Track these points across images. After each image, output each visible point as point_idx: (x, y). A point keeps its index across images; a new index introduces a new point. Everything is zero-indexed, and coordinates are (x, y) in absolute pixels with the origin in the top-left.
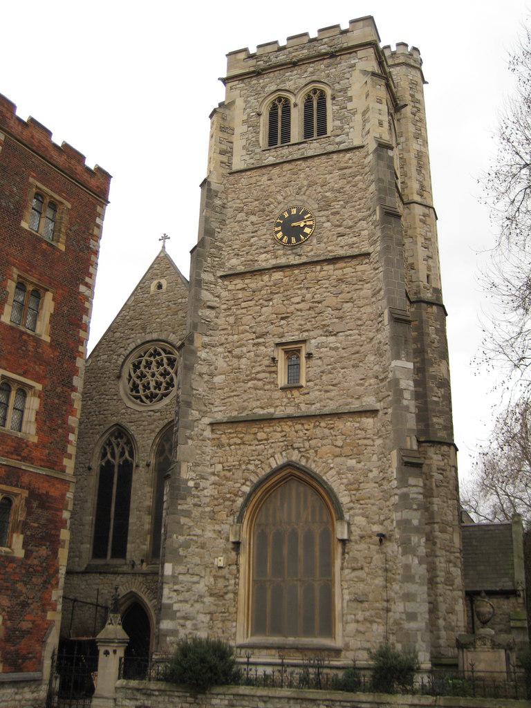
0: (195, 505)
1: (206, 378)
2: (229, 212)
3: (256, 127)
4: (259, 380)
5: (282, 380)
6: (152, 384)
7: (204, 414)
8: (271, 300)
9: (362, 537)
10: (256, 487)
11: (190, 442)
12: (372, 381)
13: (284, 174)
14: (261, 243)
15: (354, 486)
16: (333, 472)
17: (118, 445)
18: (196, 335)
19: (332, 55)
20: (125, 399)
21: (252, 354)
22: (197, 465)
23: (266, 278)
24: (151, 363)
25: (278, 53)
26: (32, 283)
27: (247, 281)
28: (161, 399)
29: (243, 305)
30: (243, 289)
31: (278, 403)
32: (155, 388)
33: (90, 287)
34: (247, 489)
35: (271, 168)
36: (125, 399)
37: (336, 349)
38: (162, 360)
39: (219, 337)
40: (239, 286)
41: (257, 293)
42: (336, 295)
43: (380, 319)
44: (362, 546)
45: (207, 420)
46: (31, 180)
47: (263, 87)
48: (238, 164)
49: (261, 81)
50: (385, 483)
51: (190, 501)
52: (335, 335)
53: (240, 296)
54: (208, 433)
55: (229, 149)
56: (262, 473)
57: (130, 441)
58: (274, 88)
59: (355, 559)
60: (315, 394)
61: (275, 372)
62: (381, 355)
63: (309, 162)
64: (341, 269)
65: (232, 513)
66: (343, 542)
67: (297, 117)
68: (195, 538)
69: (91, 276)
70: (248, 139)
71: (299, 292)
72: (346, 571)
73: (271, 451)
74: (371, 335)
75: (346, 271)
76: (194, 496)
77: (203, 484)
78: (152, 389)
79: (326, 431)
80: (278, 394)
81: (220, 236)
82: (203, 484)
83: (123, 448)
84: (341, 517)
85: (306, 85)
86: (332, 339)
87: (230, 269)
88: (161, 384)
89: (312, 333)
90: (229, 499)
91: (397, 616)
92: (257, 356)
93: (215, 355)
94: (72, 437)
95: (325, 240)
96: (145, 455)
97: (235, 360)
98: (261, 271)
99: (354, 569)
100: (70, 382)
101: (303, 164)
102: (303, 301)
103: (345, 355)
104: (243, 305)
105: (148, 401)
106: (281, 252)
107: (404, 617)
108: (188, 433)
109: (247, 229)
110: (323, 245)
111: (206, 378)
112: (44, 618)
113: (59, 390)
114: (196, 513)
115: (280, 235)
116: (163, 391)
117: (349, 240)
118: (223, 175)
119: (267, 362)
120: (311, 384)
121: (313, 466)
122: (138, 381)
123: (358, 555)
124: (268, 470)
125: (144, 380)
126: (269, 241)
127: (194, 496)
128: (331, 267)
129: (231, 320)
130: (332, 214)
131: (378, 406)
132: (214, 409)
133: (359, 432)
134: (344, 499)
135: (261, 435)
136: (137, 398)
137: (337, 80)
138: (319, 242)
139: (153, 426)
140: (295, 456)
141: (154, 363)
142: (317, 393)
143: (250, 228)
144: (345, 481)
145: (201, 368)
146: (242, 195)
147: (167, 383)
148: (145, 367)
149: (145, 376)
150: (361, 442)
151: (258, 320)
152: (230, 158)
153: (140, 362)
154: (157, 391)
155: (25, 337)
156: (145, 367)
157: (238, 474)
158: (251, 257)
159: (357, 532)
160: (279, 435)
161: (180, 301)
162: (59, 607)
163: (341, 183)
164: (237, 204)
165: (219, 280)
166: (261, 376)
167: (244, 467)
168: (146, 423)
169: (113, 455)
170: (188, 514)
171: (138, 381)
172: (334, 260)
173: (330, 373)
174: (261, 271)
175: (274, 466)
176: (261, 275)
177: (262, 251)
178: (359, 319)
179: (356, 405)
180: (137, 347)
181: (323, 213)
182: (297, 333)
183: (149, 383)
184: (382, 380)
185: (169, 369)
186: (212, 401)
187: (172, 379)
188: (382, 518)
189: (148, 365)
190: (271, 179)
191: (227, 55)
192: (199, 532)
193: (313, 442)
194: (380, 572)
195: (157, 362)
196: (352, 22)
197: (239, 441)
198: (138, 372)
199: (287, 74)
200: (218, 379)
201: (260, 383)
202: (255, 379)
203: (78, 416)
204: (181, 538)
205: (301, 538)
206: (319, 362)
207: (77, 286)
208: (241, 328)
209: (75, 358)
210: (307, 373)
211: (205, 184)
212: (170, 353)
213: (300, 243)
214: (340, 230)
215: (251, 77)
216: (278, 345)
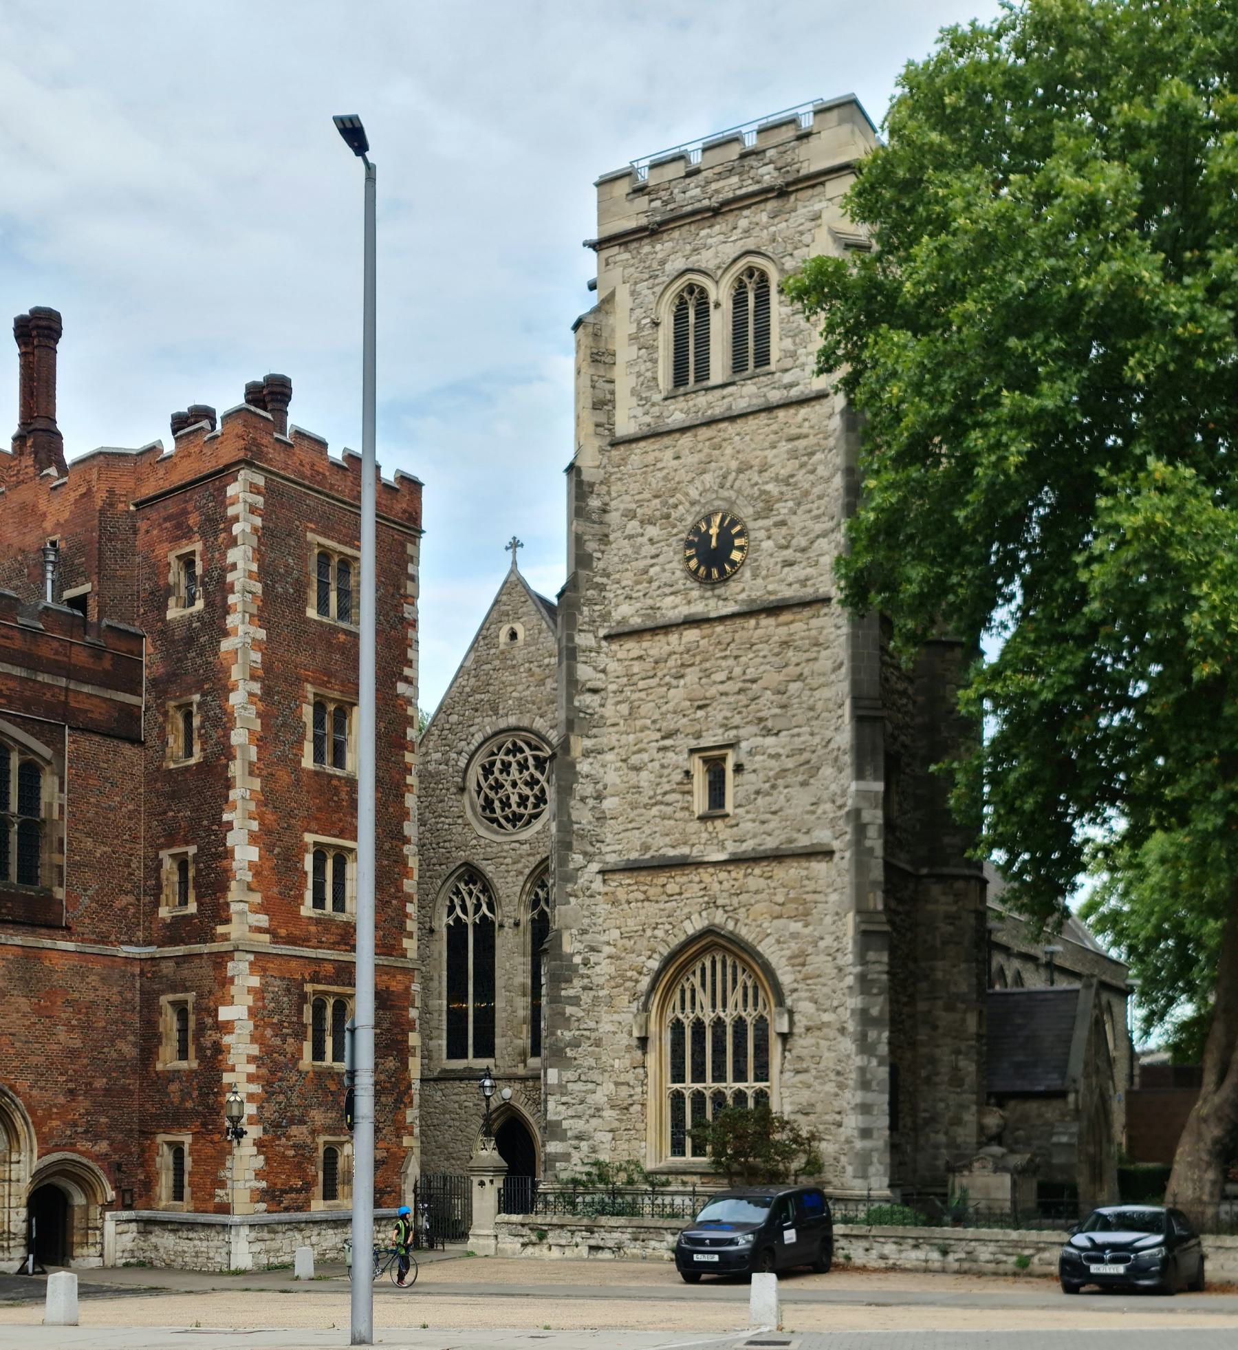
0: (584, 988)
1: (591, 802)
2: (614, 518)
3: (652, 348)
4: (668, 804)
5: (700, 801)
6: (514, 799)
7: (589, 857)
8: (682, 676)
9: (808, 1029)
10: (668, 961)
11: (572, 900)
12: (828, 806)
13: (700, 446)
14: (666, 577)
15: (800, 960)
16: (771, 940)
17: (470, 893)
18: (572, 739)
19: (782, 193)
20: (475, 823)
21: (656, 764)
22: (584, 932)
23: (673, 638)
24: (510, 764)
25: (688, 181)
26: (333, 700)
27: (645, 644)
28: (529, 822)
29: (641, 685)
30: (640, 658)
31: (694, 839)
32: (519, 805)
33: (410, 681)
34: (655, 964)
35: (677, 435)
36: (475, 823)
37: (777, 756)
38: (526, 760)
39: (608, 737)
40: (636, 653)
41: (662, 665)
42: (779, 669)
43: (840, 712)
44: (809, 1041)
45: (595, 867)
46: (310, 536)
47: (663, 263)
48: (625, 425)
49: (658, 247)
50: (839, 955)
51: (577, 982)
52: (777, 734)
53: (636, 669)
54: (598, 885)
55: (609, 397)
56: (675, 942)
57: (487, 888)
58: (678, 264)
59: (800, 1058)
60: (747, 826)
61: (690, 793)
62: (840, 771)
63: (739, 425)
64: (787, 624)
65: (634, 997)
66: (785, 1037)
67: (720, 325)
68: (587, 1033)
69: (409, 663)
70: (639, 375)
71: (724, 663)
72: (787, 1075)
73: (686, 910)
74: (829, 734)
75: (794, 627)
76: (582, 977)
77: (593, 958)
78: (514, 807)
79: (762, 883)
80: (695, 826)
81: (601, 565)
82: (593, 958)
83: (478, 899)
84: (780, 1002)
85: (735, 261)
86: (770, 740)
87: (619, 623)
88: (527, 798)
89: (742, 732)
90: (630, 979)
91: (849, 1132)
92: (663, 766)
93: (603, 766)
94: (411, 908)
95: (764, 573)
96: (513, 911)
97: (633, 774)
98: (666, 628)
99: (798, 1072)
100: (401, 831)
101: (729, 429)
102: (729, 679)
103: (790, 765)
104: (641, 685)
105: (509, 826)
106: (695, 594)
107: (856, 1133)
108: (569, 888)
109: (644, 552)
110: (760, 581)
111: (591, 802)
112: (399, 1145)
113: (387, 846)
114: (586, 998)
115: (693, 564)
116: (530, 810)
117: (798, 572)
118: (601, 451)
119: (678, 776)
120: (740, 811)
121: (744, 932)
122: (492, 794)
123: (804, 1053)
124: (682, 938)
125: (501, 793)
126: (678, 574)
127: (582, 977)
128: (771, 621)
129: (624, 709)
130: (776, 525)
131: (836, 845)
132: (605, 849)
133: (806, 882)
134: (786, 978)
135: (672, 888)
136: (493, 820)
137: (789, 248)
138: (755, 576)
139: (520, 866)
140: (719, 917)
141: (514, 766)
142: (750, 825)
143: (650, 550)
144: (788, 953)
145: (584, 788)
146: (634, 488)
147: (536, 797)
148: (501, 772)
149: (502, 786)
150: (809, 897)
151: (664, 709)
152: (610, 415)
153: (493, 764)
154: (522, 810)
155: (335, 782)
156: (501, 772)
157: (642, 944)
158: (650, 602)
159: (801, 1022)
160: (696, 887)
161: (546, 661)
162: (417, 1131)
163: (792, 465)
164: (627, 503)
165: (604, 643)
166: (669, 798)
167: (649, 933)
168: (509, 860)
169: (465, 911)
170: (575, 1001)
171: (492, 794)
172: (775, 609)
173: (768, 794)
174: (666, 628)
175: (691, 931)
176: (666, 634)
177: (667, 590)
178: (812, 709)
179: (803, 841)
180: (486, 740)
181: (761, 523)
182: (721, 731)
183: (508, 798)
184: (840, 807)
185: (538, 775)
186: (601, 837)
187: (543, 791)
188: (835, 1003)
189: (506, 767)
190: (678, 458)
191: (598, 185)
192: (592, 1025)
193: (743, 898)
194: (832, 1076)
195: (519, 763)
196: (822, 111)
197: (642, 897)
198: (491, 780)
199: (703, 233)
200: (609, 804)
201: (669, 810)
202: (662, 803)
203: (416, 877)
204: (568, 1035)
205: (729, 1030)
206: (753, 777)
207: (394, 684)
208: (639, 723)
209: (403, 796)
210: (735, 794)
211: (572, 469)
212: (537, 748)
213: (724, 579)
214: (788, 554)
215: (641, 239)
216: (692, 751)
